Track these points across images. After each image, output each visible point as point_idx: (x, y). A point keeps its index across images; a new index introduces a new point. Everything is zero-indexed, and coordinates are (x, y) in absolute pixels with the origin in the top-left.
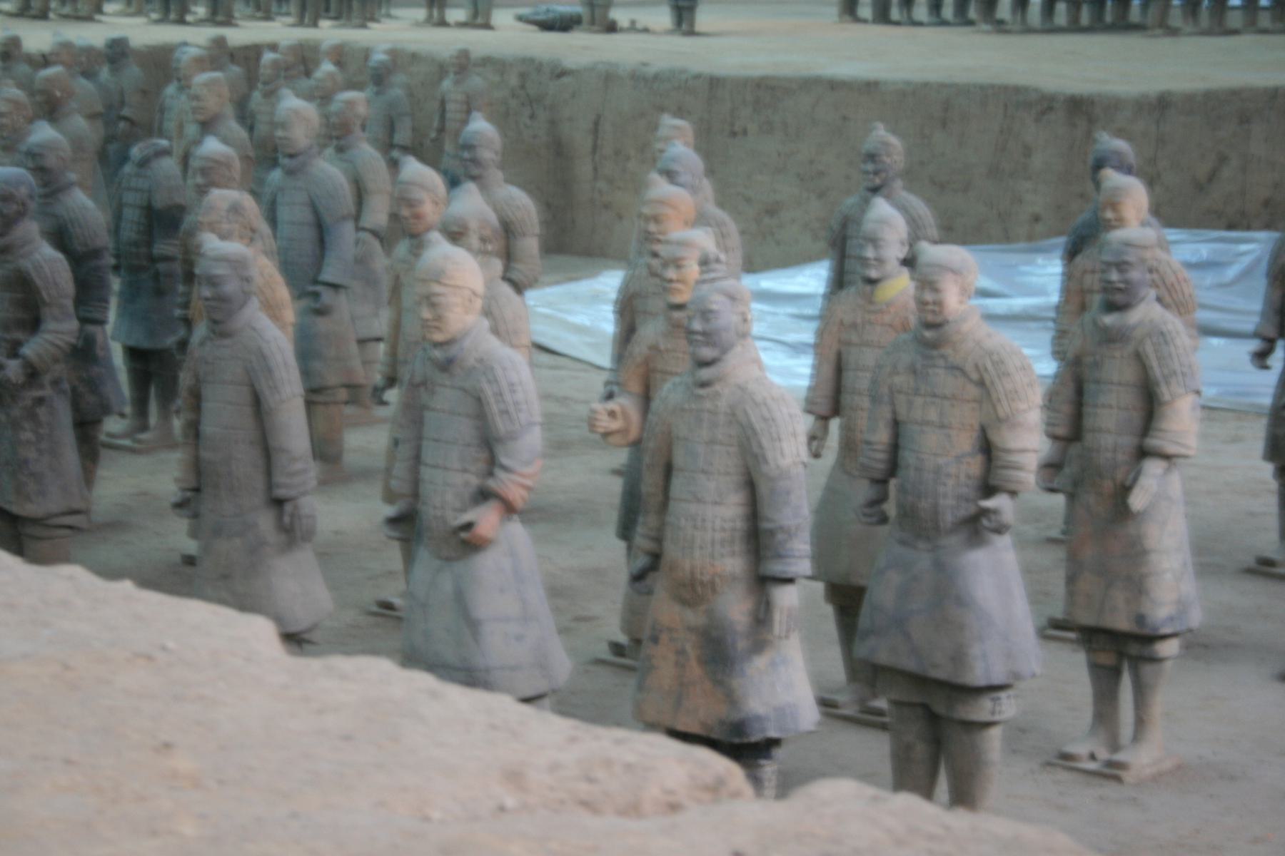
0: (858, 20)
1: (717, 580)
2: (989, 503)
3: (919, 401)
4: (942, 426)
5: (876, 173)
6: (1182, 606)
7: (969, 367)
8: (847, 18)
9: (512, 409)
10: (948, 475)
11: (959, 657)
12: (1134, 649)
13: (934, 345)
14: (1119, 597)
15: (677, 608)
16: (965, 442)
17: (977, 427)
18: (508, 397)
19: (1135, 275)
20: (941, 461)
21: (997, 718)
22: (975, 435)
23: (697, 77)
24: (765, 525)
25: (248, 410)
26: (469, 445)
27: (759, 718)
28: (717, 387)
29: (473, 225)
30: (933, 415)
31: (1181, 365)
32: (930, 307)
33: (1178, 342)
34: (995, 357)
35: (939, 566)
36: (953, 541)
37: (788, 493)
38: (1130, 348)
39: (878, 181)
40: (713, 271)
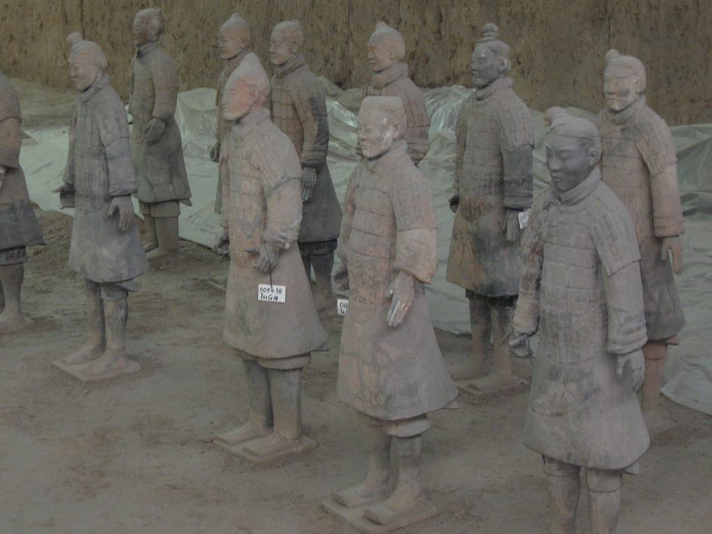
1: (482, 207)
15: (464, 221)
24: (506, 178)
28: (486, 100)
40: (488, 36)
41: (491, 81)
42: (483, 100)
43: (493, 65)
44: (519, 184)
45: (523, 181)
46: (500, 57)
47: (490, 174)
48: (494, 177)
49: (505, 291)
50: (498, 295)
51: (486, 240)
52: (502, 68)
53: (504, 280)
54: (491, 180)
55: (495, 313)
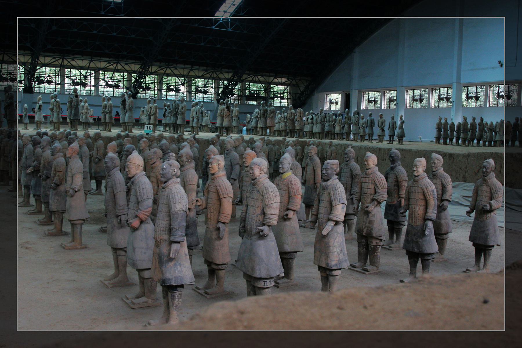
0: (439, 143)
1: (161, 240)
2: (262, 228)
3: (250, 199)
4: (254, 207)
5: (347, 157)
6: (340, 262)
7: (260, 191)
8: (437, 143)
9: (142, 195)
10: (254, 220)
11: (253, 269)
12: (328, 272)
13: (254, 185)
14: (323, 258)
16: (259, 211)
17: (262, 207)
18: (142, 192)
19: (329, 172)
20: (253, 216)
21: (265, 287)
22: (261, 209)
23: (377, 148)
25: (113, 194)
26: (135, 203)
27: (169, 279)
28: (166, 189)
29: (184, 155)
30: (252, 204)
31: (339, 196)
32: (251, 174)
33: (339, 190)
34: (267, 189)
35: (251, 244)
36: (255, 237)
37: (177, 218)
38: (328, 191)
39: (348, 159)
41: (169, 180)
42: (165, 188)
43: (169, 172)
44: (176, 230)
45: (179, 228)
46: (173, 168)
47: (166, 225)
48: (167, 226)
49: (171, 283)
50: (167, 285)
51: (163, 257)
52: (174, 173)
53: (170, 277)
54: (166, 227)
55: (170, 294)
